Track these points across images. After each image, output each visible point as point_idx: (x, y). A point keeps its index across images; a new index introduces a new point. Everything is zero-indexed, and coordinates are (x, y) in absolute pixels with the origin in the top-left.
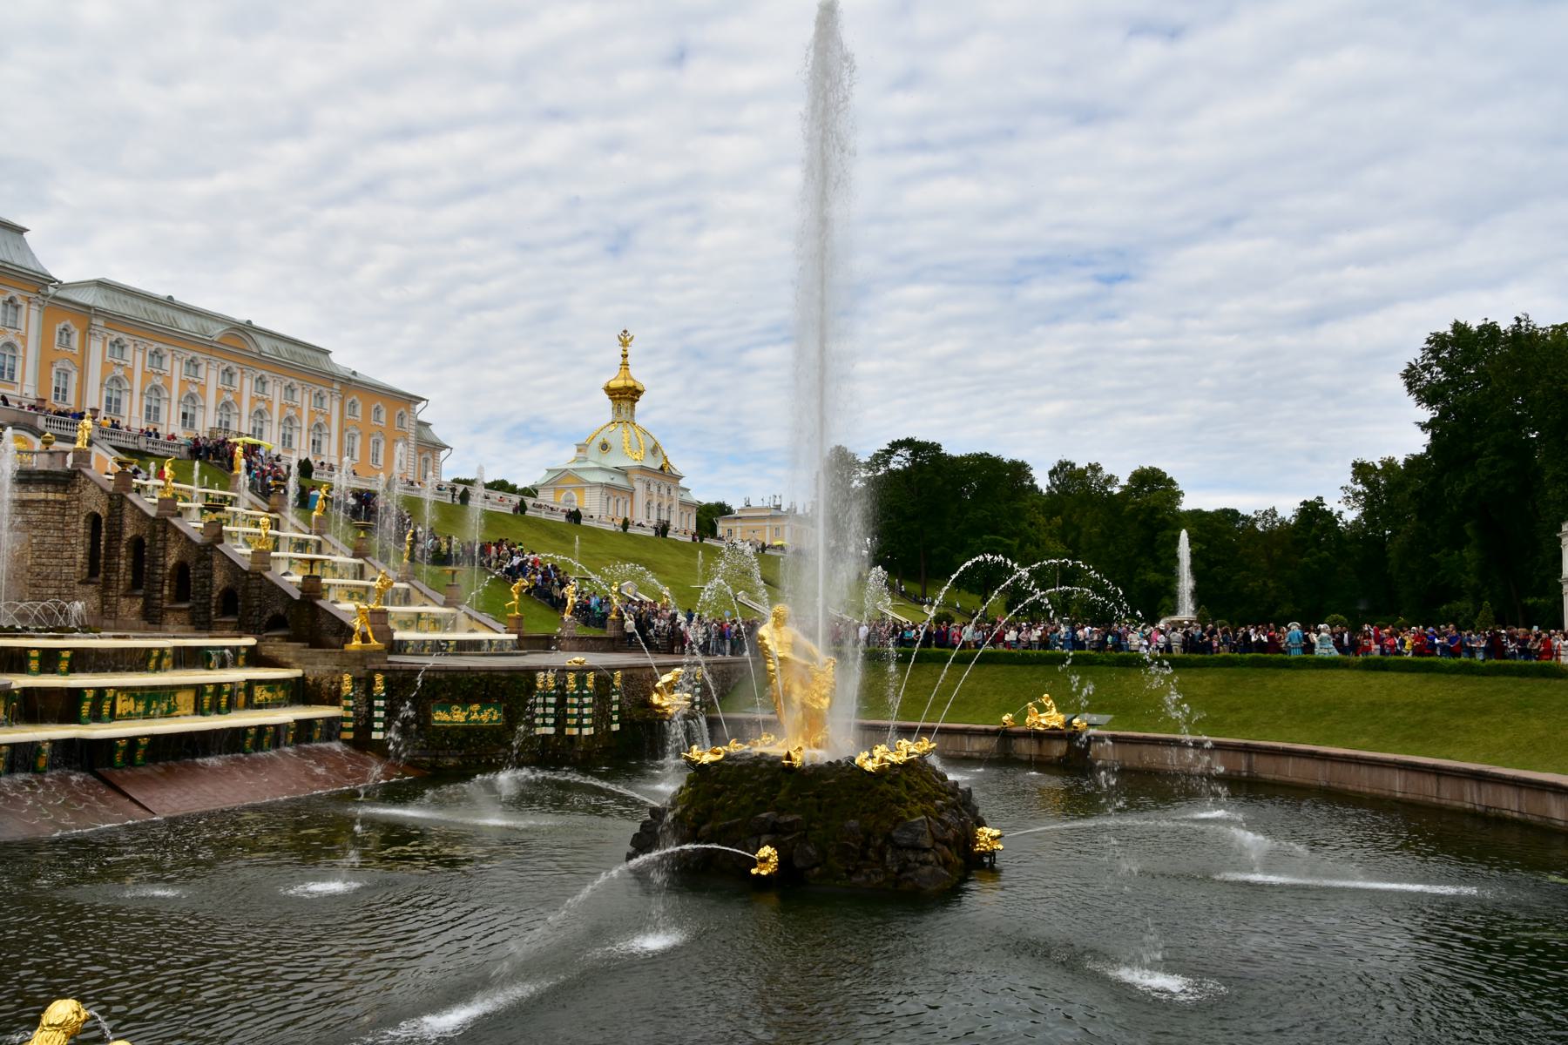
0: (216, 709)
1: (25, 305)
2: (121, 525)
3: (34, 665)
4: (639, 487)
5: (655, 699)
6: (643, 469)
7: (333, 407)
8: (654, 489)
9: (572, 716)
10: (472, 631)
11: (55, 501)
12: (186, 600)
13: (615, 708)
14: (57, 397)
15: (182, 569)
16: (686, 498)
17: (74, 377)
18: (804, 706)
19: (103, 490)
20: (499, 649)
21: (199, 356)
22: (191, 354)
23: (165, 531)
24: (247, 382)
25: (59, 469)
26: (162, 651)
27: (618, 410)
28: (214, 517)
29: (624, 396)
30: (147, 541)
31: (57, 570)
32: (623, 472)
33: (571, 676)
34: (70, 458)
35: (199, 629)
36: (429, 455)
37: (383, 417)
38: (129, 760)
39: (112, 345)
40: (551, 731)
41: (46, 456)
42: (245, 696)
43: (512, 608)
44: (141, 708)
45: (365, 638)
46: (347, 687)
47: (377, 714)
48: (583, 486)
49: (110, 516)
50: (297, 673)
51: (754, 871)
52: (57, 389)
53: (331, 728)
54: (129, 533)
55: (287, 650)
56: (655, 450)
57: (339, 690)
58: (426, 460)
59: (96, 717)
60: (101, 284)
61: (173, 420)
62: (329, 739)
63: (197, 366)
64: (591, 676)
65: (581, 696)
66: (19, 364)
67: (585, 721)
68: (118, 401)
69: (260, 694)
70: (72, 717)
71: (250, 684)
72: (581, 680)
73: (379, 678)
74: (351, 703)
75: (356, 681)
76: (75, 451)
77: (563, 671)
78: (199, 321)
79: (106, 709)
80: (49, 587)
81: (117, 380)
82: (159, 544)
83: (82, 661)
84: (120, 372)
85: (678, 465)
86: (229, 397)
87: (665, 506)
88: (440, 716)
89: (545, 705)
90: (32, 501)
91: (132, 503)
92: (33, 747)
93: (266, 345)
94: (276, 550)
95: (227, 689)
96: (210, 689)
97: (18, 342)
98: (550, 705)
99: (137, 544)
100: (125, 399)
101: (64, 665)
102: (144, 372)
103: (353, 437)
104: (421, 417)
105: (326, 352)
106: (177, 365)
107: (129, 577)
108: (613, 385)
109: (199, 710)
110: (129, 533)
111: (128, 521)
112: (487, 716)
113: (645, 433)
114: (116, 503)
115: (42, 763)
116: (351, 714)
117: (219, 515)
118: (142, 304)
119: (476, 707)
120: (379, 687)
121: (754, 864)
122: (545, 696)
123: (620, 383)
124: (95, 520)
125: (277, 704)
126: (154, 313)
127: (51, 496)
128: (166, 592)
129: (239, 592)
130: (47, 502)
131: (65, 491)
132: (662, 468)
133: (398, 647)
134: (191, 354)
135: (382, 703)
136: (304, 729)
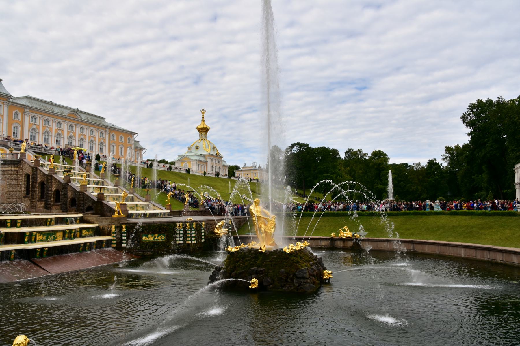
0: (70, 238)
1: (2, 105)
2: (37, 177)
3: (9, 225)
4: (209, 161)
5: (216, 231)
6: (210, 155)
7: (106, 137)
8: (214, 161)
9: (188, 237)
10: (155, 210)
11: (14, 170)
12: (59, 202)
13: (203, 234)
14: (14, 135)
15: (57, 192)
16: (224, 164)
17: (20, 129)
18: (265, 232)
19: (30, 166)
20: (165, 215)
21: (61, 121)
22: (58, 120)
23: (51, 179)
24: (77, 129)
25: (15, 159)
26: (51, 219)
27: (201, 135)
28: (67, 174)
29: (204, 131)
30: (45, 183)
31: (15, 193)
32: (203, 156)
33: (188, 224)
34: (19, 156)
35: (63, 211)
36: (138, 152)
37: (123, 140)
38: (41, 256)
39: (32, 118)
40: (182, 242)
41: (11, 155)
42: (80, 233)
43: (168, 202)
44: (45, 238)
45: (119, 213)
46: (113, 230)
47: (123, 238)
48: (190, 161)
49: (33, 174)
50: (97, 225)
51: (250, 287)
52: (14, 133)
53: (108, 243)
54: (39, 180)
55: (93, 218)
56: (214, 148)
57: (111, 231)
58: (138, 154)
59: (30, 241)
60: (28, 98)
61: (53, 142)
62: (108, 247)
63: (60, 124)
64: (194, 224)
65: (191, 231)
67: (193, 239)
68: (35, 136)
69: (84, 232)
70: (22, 242)
71: (81, 229)
72: (191, 225)
73: (124, 226)
74: (115, 235)
75: (116, 227)
76: (21, 153)
77: (186, 222)
78: (61, 109)
79: (33, 239)
80: (13, 199)
81: (34, 129)
82: (50, 184)
83: (25, 223)
84: (35, 127)
85: (222, 153)
86: (72, 134)
87: (218, 167)
88: (145, 238)
89: (179, 234)
90: (7, 170)
91: (40, 170)
92: (9, 252)
93: (83, 117)
94: (89, 184)
95: (73, 231)
96: (68, 231)
98: (181, 234)
99: (42, 184)
100: (37, 136)
101: (19, 225)
102: (43, 126)
103: (113, 146)
104: (136, 139)
105: (104, 118)
106: (54, 124)
107: (40, 195)
108: (199, 127)
109: (64, 238)
110: (39, 180)
111: (39, 176)
112: (160, 238)
113: (210, 143)
114: (35, 170)
115: (12, 257)
116: (115, 238)
117: (69, 173)
118: (42, 104)
119: (156, 235)
120: (124, 229)
121: (250, 284)
122: (180, 231)
123: (202, 126)
124: (28, 176)
125: (90, 236)
126: (46, 107)
127: (13, 168)
128: (52, 199)
129: (77, 199)
130: (11, 170)
131: (17, 167)
133: (130, 216)
134: (58, 120)
135: (125, 234)
136: (99, 244)
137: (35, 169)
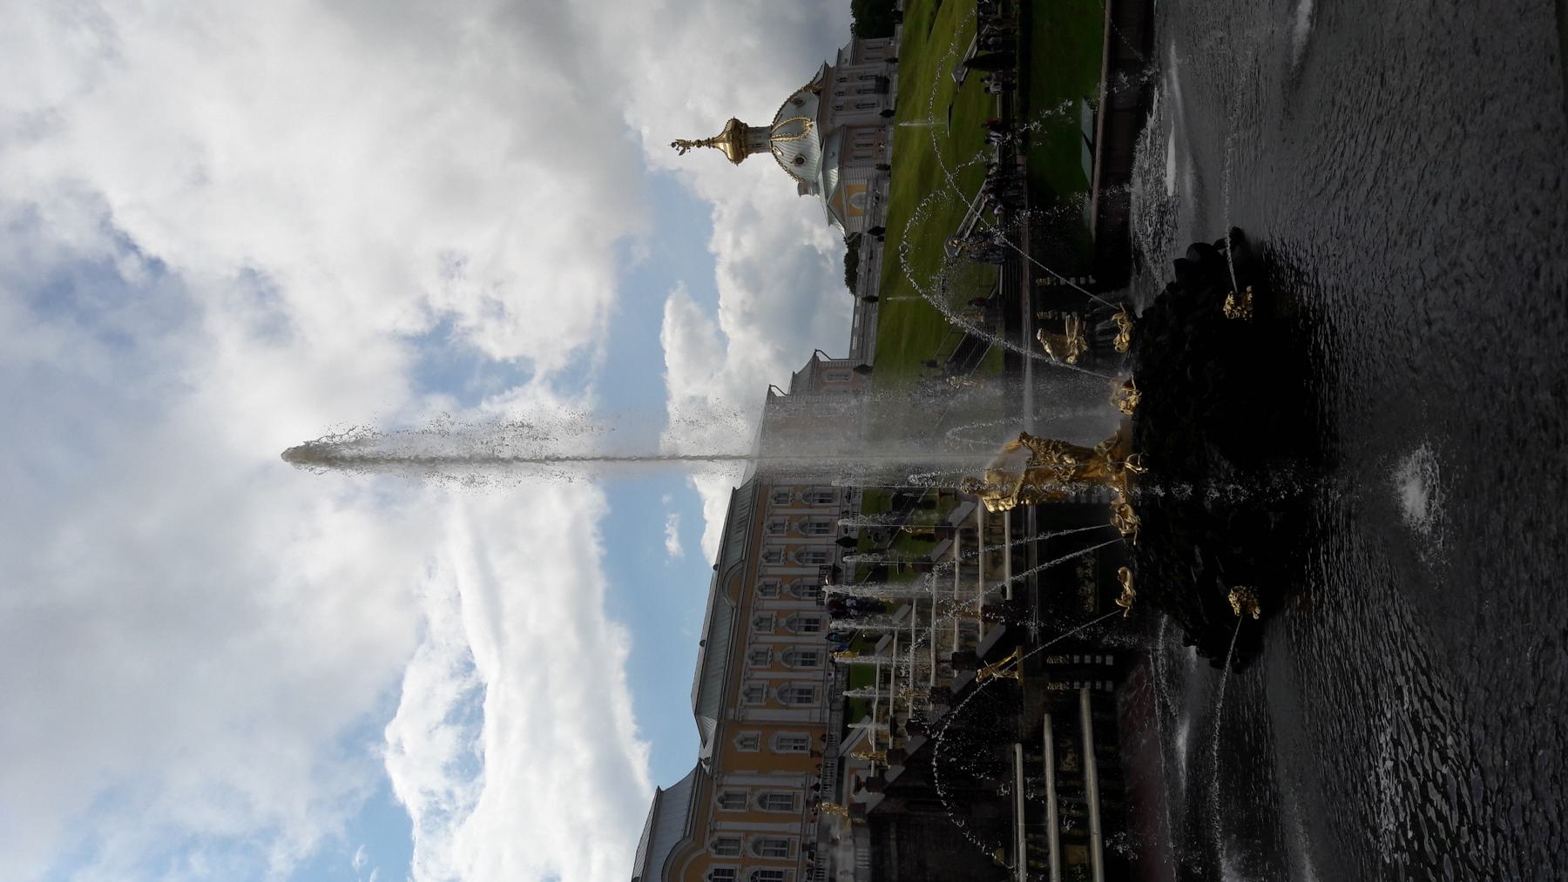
4: (840, 120)
8: (841, 100)
16: (848, 55)
21: (751, 619)
22: (751, 625)
29: (743, 140)
32: (825, 140)
50: (1047, 718)
53: (1102, 703)
63: (762, 620)
66: (776, 792)
71: (1058, 773)
75: (1054, 680)
87: (860, 84)
93: (737, 553)
97: (758, 794)
100: (797, 685)
109: (1086, 840)
116: (1088, 684)
127: (893, 836)
130: (899, 840)
132: (818, 93)
137: (890, 791)
